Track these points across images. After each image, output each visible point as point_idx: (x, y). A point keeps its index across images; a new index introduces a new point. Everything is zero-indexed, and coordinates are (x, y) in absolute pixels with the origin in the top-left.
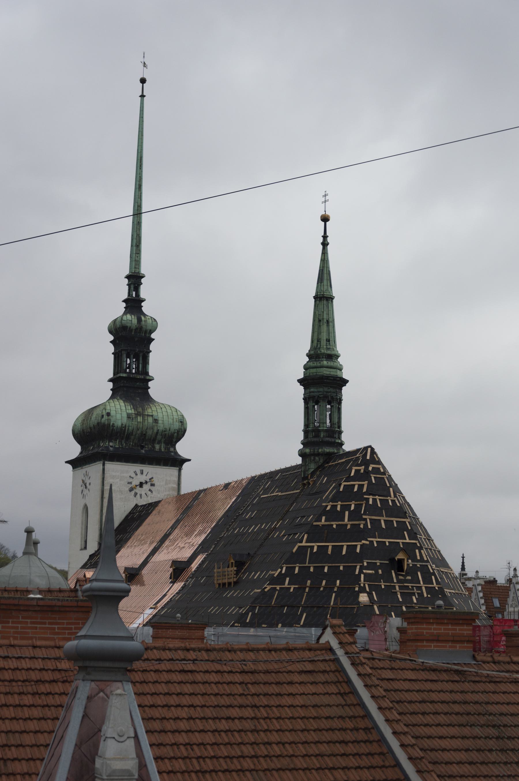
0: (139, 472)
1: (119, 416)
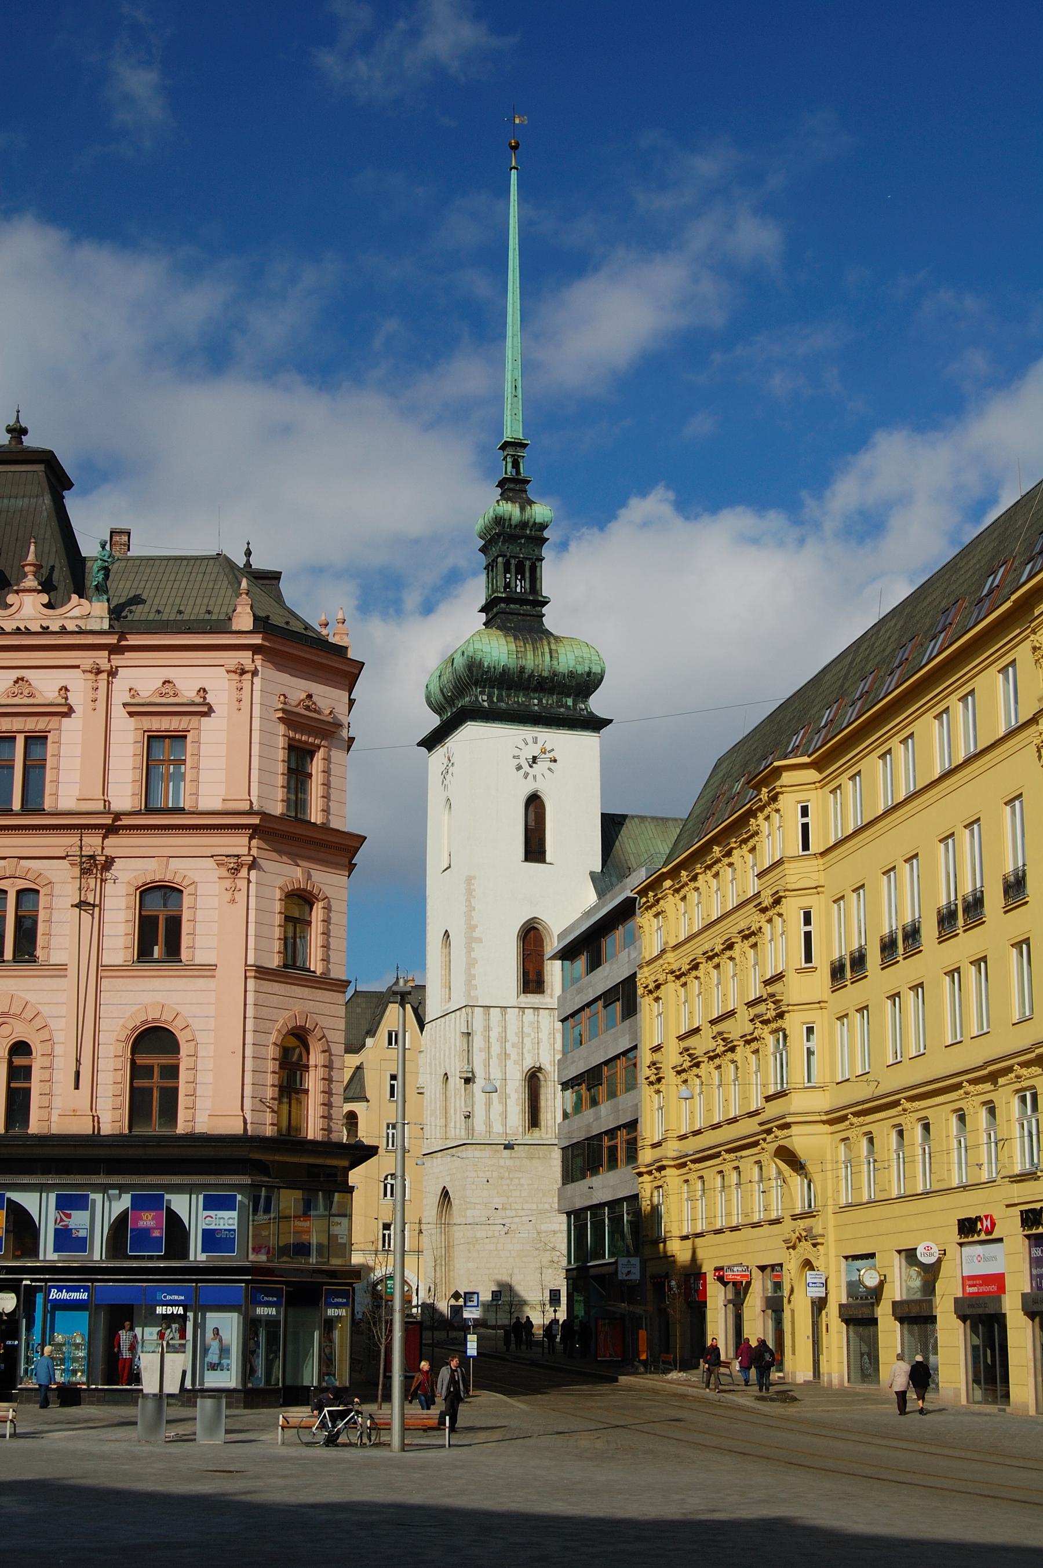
0: (530, 741)
1: (495, 654)
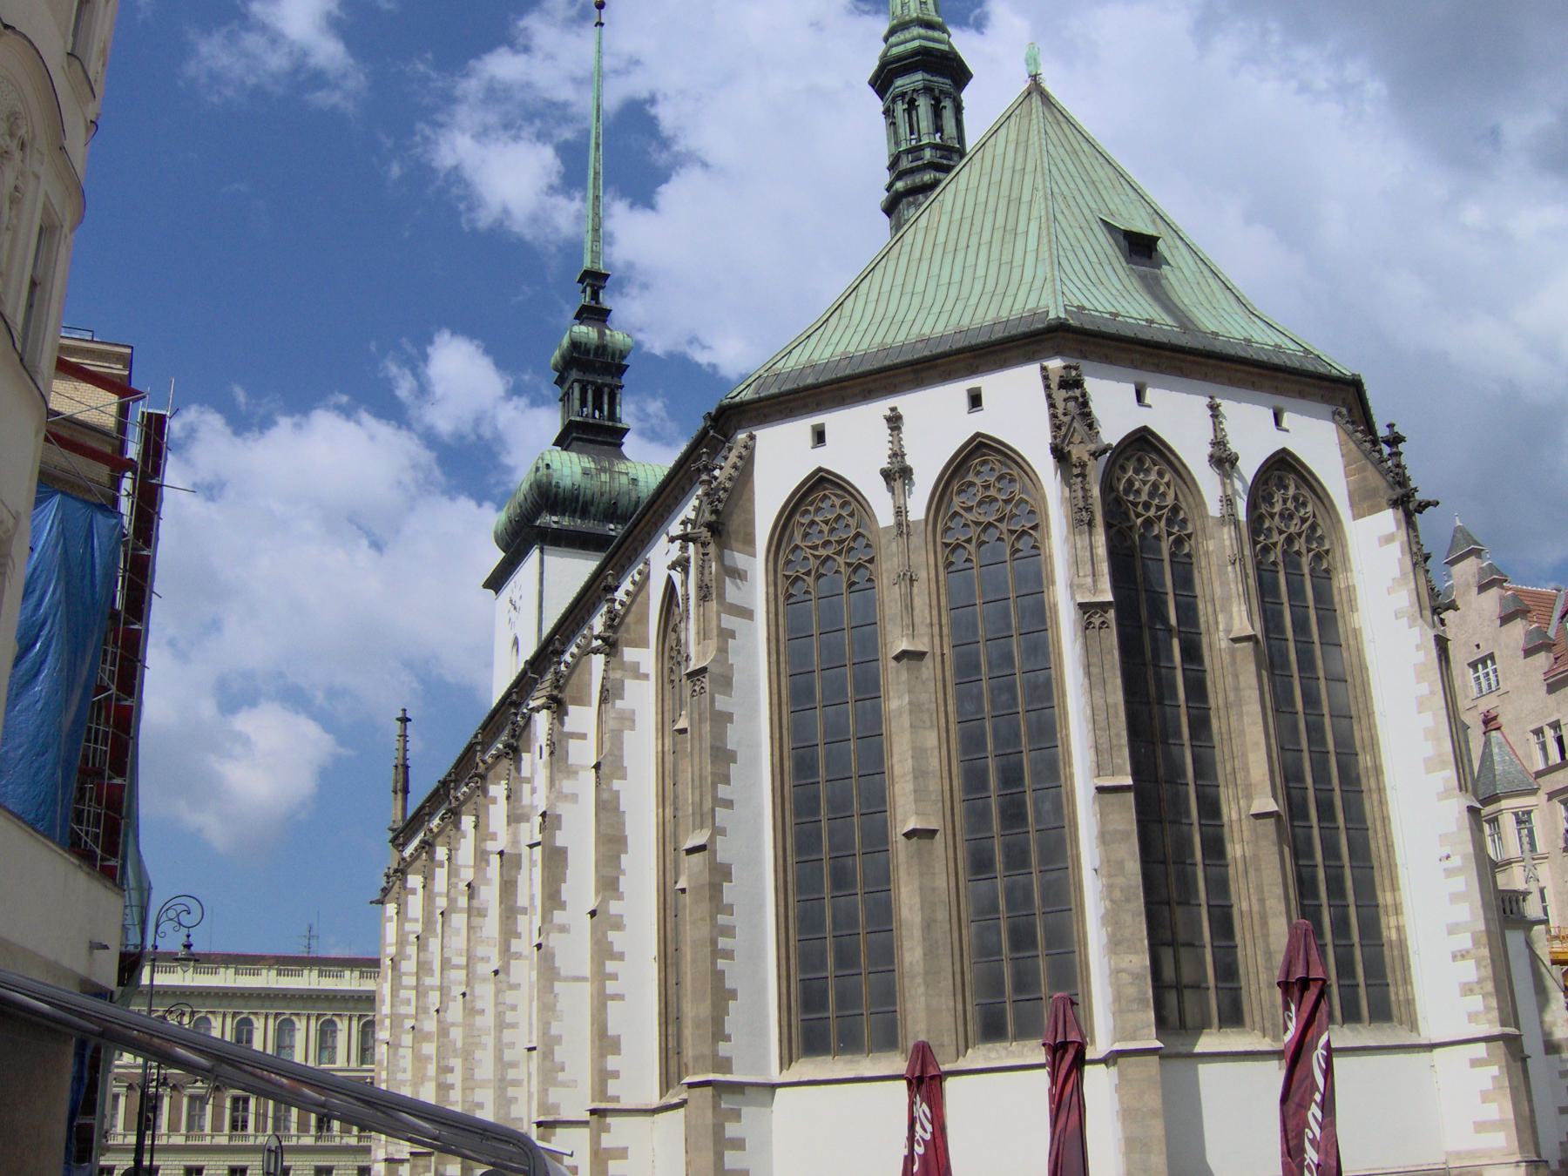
1: (567, 471)
